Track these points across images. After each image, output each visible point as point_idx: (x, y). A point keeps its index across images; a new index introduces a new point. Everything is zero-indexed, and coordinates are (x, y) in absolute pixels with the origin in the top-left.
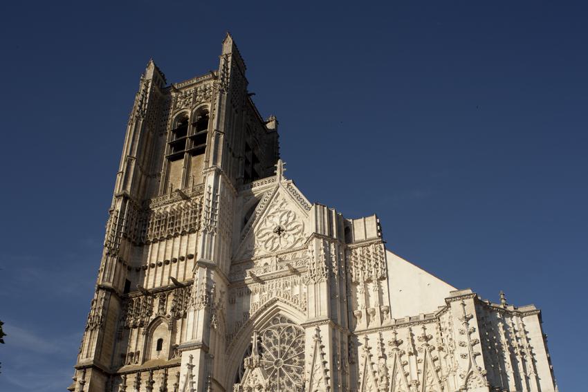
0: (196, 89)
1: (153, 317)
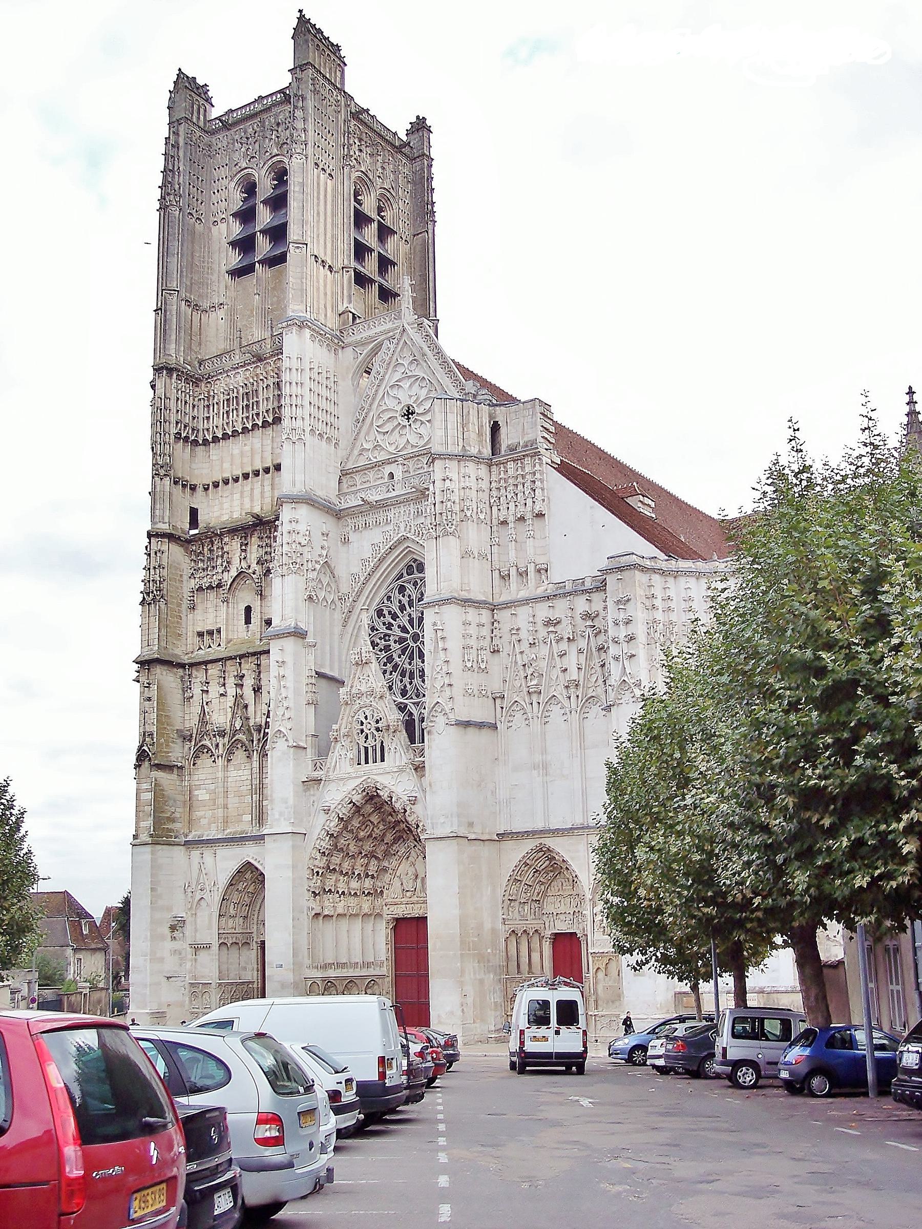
1: (234, 573)
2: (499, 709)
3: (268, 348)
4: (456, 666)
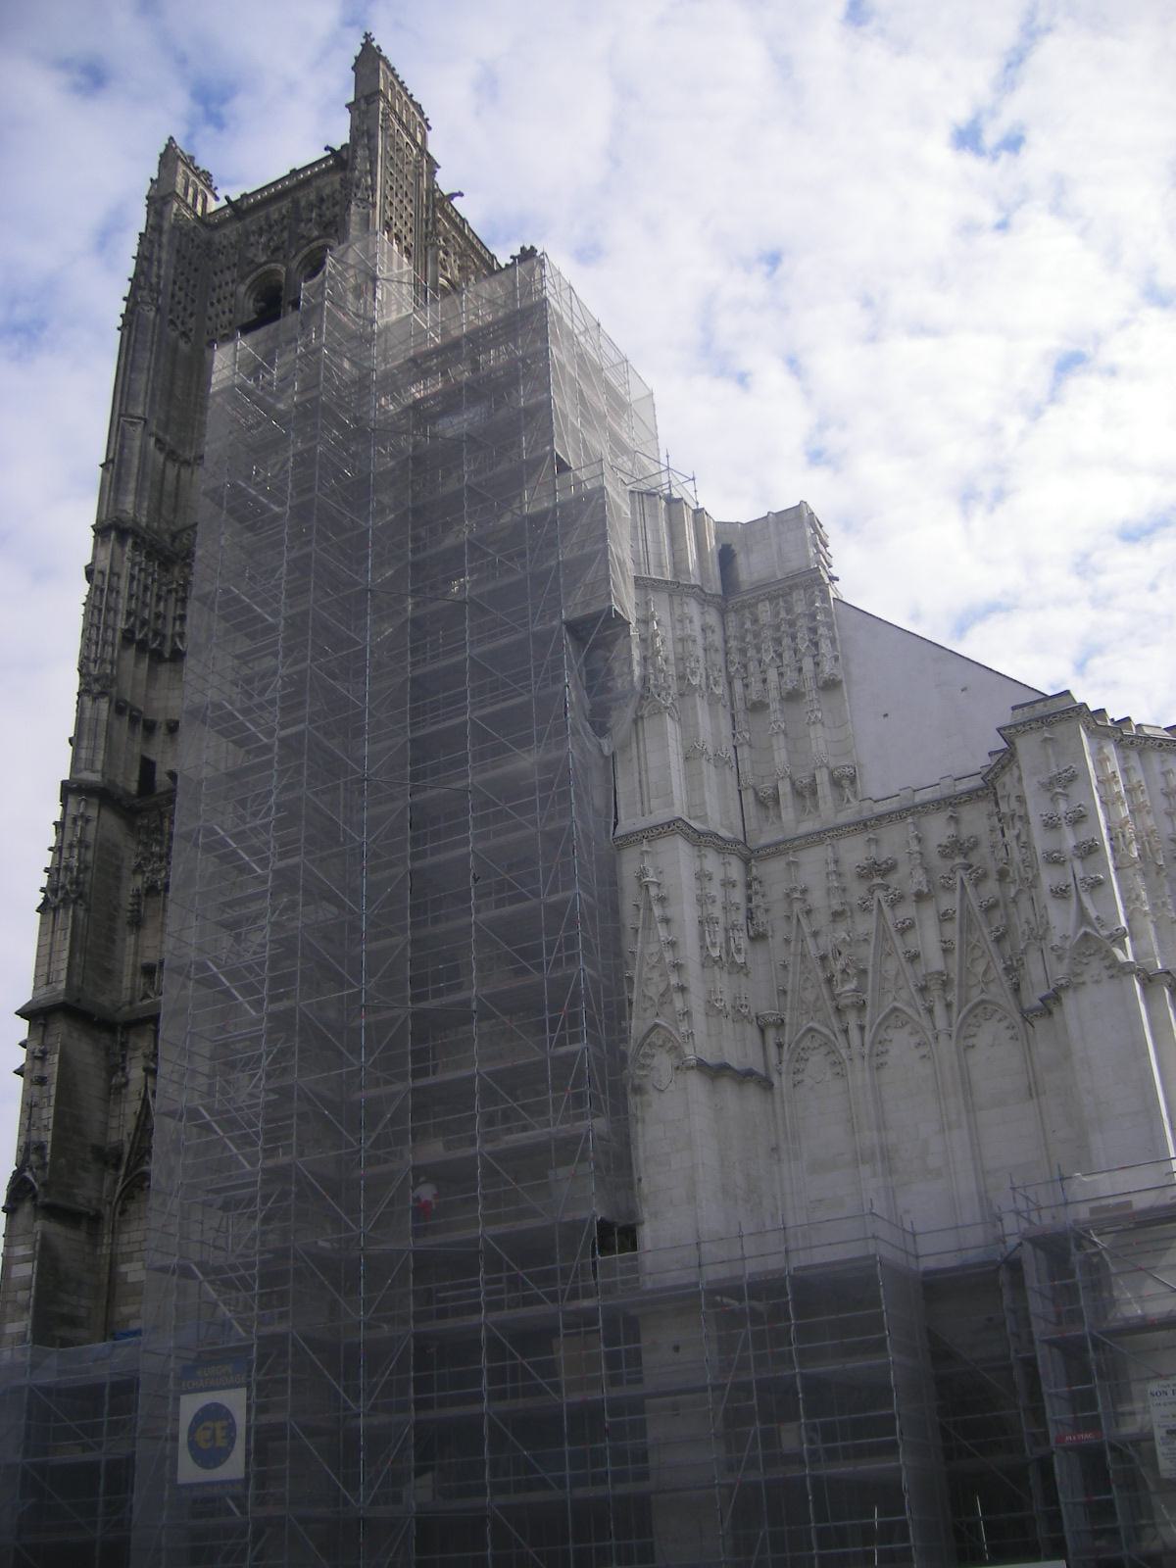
0: (296, 203)
2: (772, 1050)
4: (690, 952)
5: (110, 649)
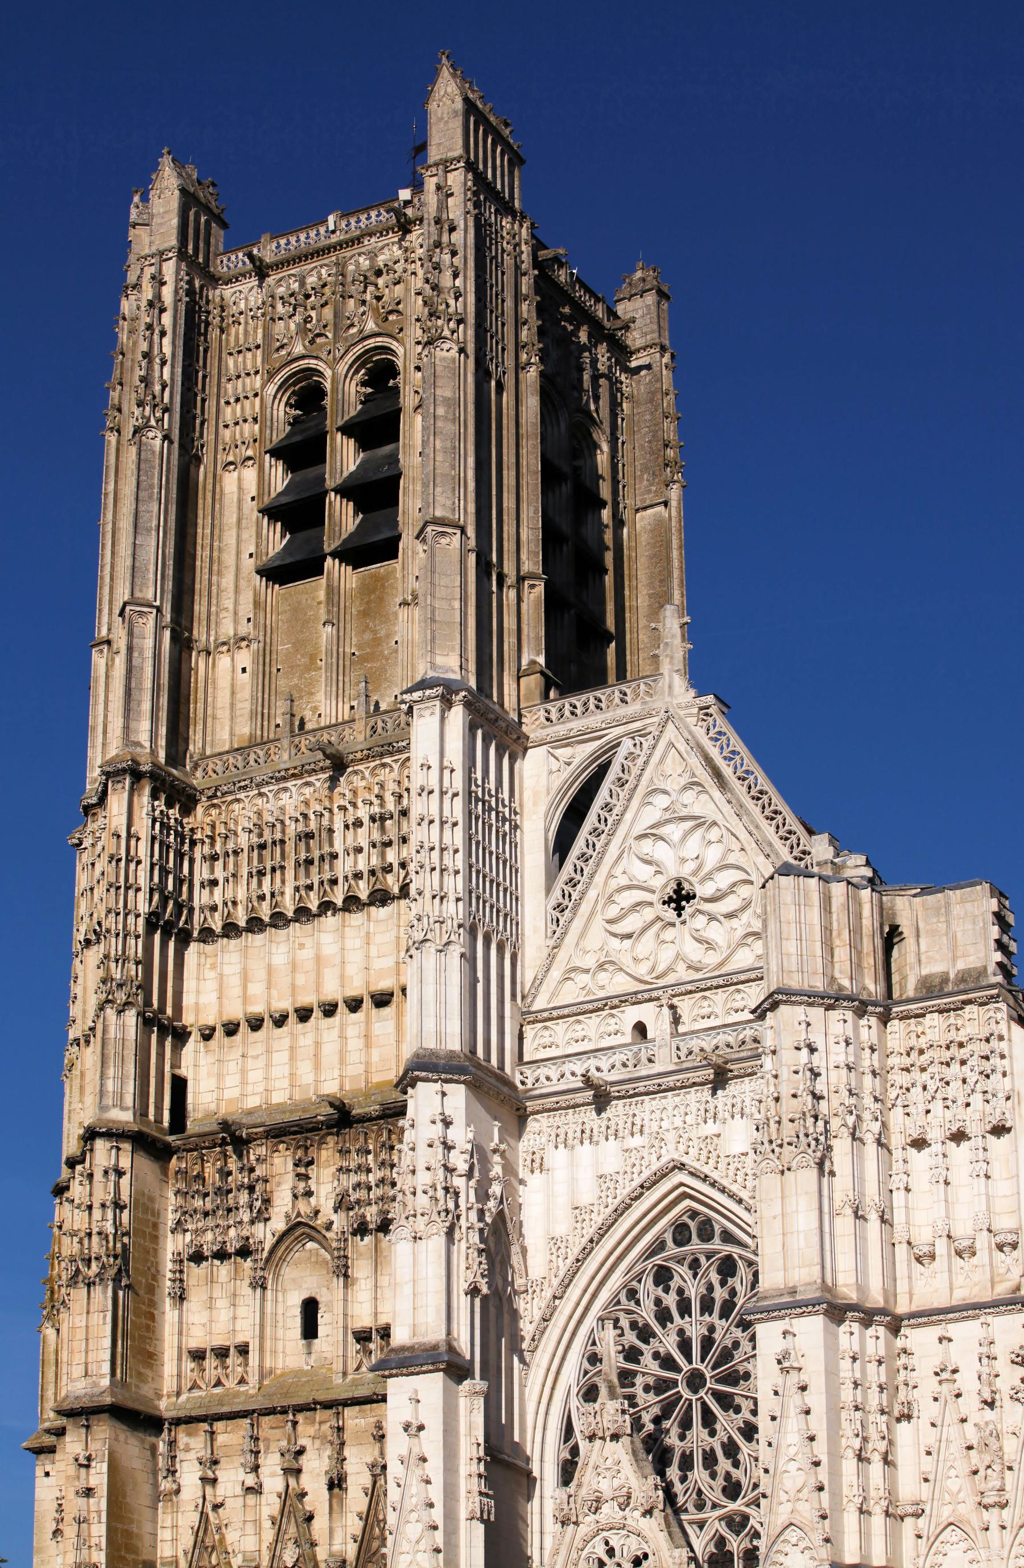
0: (341, 267)
1: (278, 1224)
3: (357, 738)
5: (133, 942)
